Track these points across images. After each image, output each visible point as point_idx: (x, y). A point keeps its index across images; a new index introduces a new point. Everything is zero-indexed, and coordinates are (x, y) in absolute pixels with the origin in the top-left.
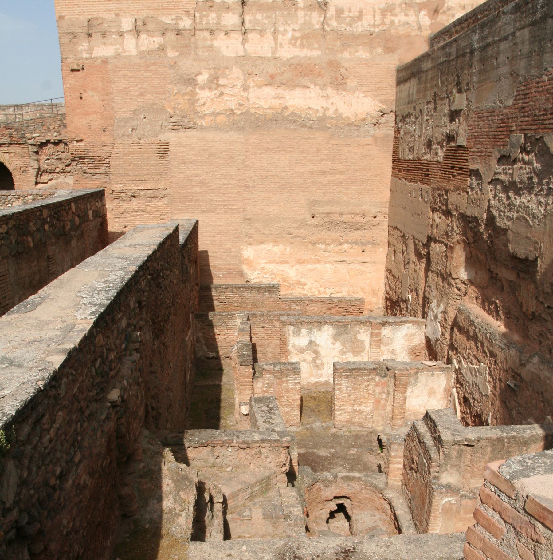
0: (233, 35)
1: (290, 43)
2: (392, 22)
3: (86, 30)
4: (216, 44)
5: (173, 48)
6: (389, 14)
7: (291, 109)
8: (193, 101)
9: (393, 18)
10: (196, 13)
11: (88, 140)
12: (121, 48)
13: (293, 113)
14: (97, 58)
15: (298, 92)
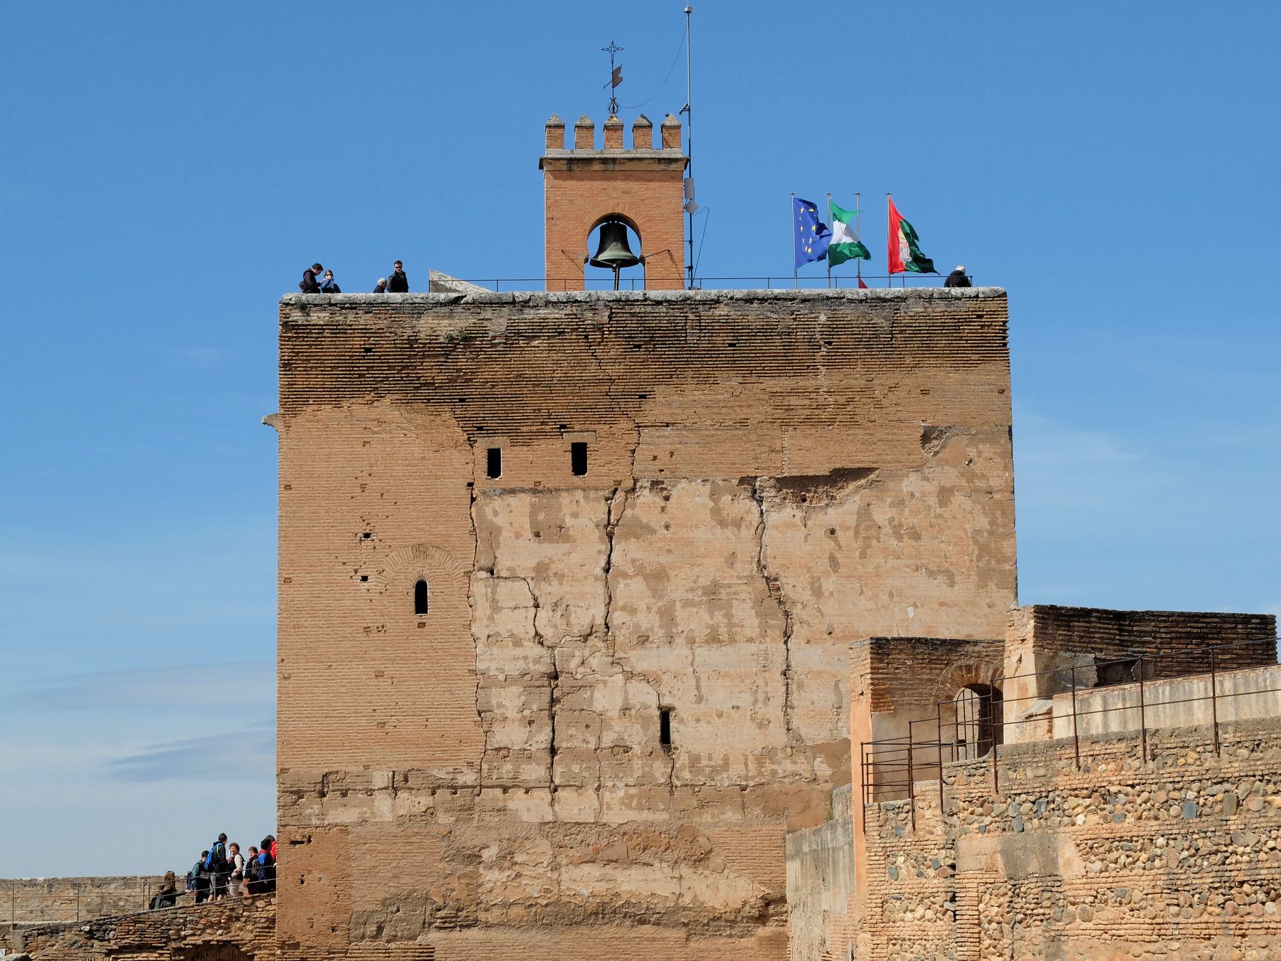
0: (536, 793)
1: (623, 803)
2: (774, 773)
3: (318, 787)
4: (511, 805)
5: (447, 811)
6: (768, 761)
7: (625, 897)
8: (474, 884)
9: (775, 767)
10: (483, 764)
11: (309, 944)
12: (369, 812)
13: (627, 902)
14: (330, 826)
15: (635, 872)
